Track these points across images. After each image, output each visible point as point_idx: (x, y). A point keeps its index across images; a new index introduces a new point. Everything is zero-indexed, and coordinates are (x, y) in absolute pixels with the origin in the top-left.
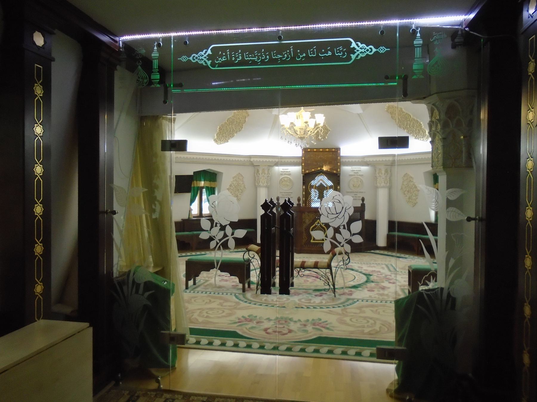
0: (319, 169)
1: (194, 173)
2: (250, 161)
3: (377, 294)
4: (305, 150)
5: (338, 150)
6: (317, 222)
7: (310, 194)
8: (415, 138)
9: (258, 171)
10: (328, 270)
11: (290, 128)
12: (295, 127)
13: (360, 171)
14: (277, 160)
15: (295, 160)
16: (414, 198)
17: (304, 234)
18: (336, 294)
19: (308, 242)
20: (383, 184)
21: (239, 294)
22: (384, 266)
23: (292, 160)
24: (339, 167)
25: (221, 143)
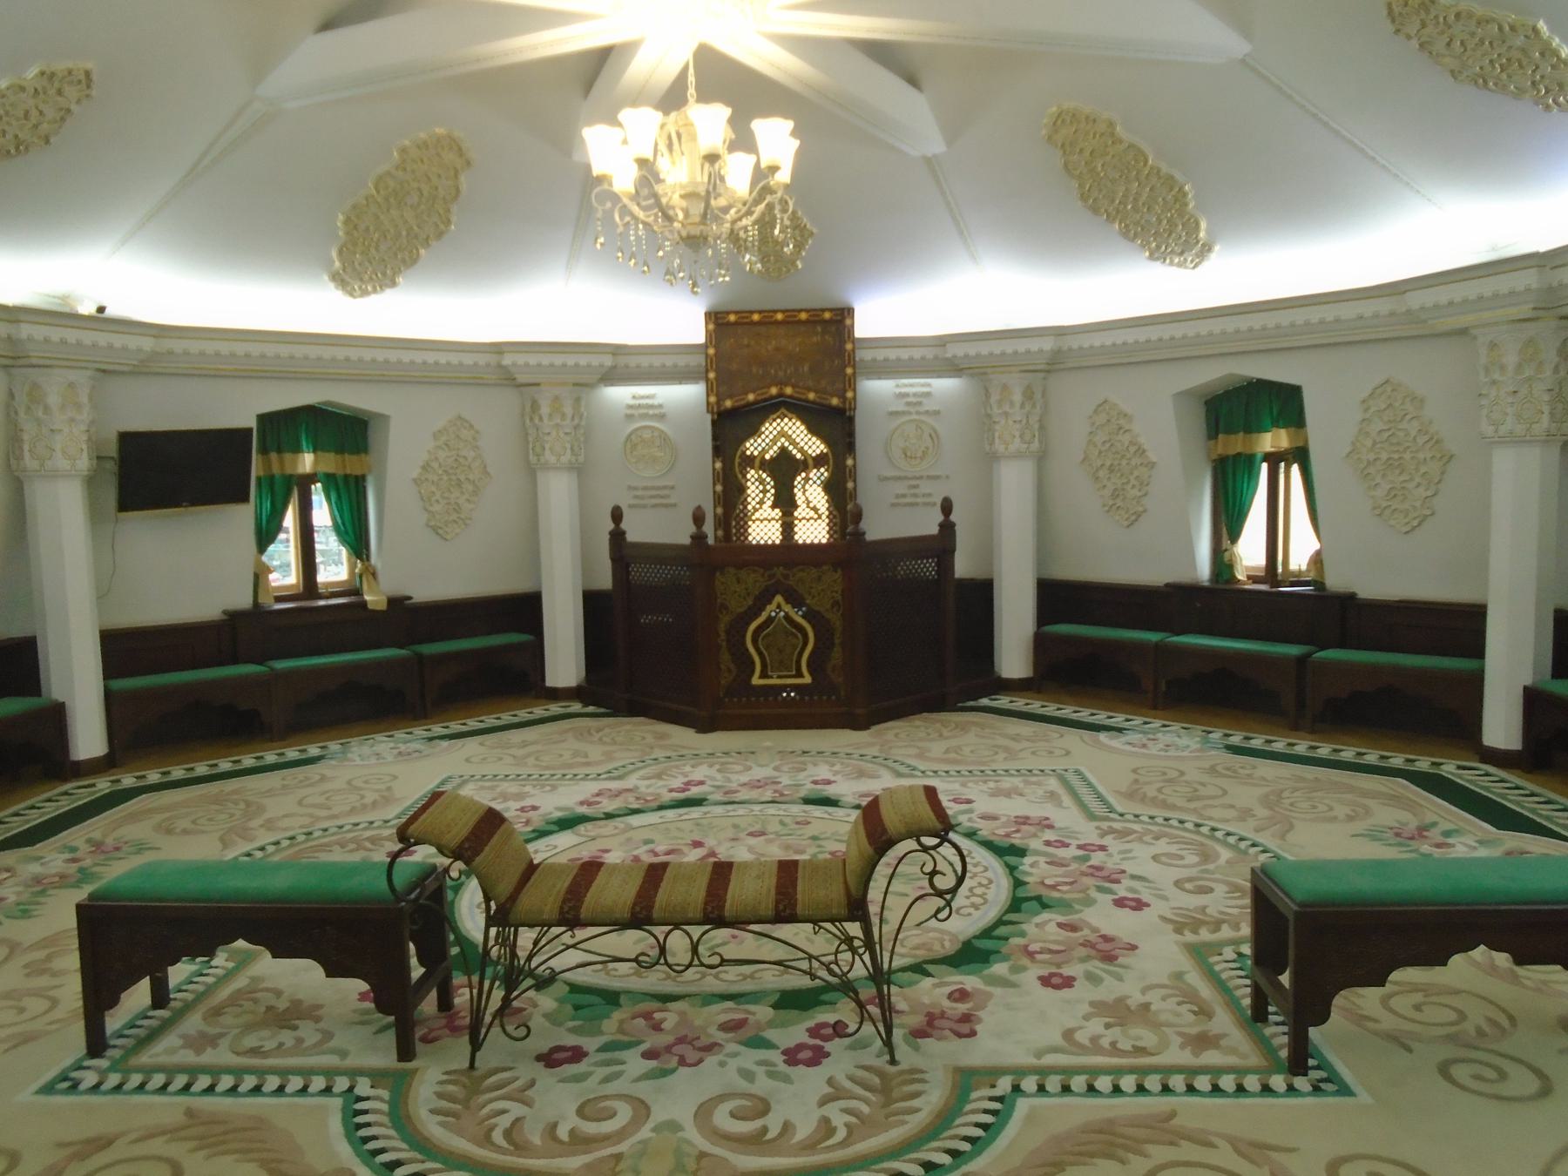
0: (774, 391)
1: (264, 419)
2: (500, 366)
3: (1099, 1008)
4: (716, 318)
5: (843, 315)
6: (773, 606)
7: (742, 489)
8: (1152, 257)
9: (535, 406)
10: (854, 929)
11: (636, 197)
12: (659, 189)
13: (928, 394)
14: (608, 361)
15: (682, 361)
16: (1135, 492)
17: (725, 657)
18: (898, 1034)
19: (742, 685)
20: (1016, 444)
21: (377, 1077)
22: (1053, 784)
23: (669, 361)
24: (851, 383)
25: (365, 293)
